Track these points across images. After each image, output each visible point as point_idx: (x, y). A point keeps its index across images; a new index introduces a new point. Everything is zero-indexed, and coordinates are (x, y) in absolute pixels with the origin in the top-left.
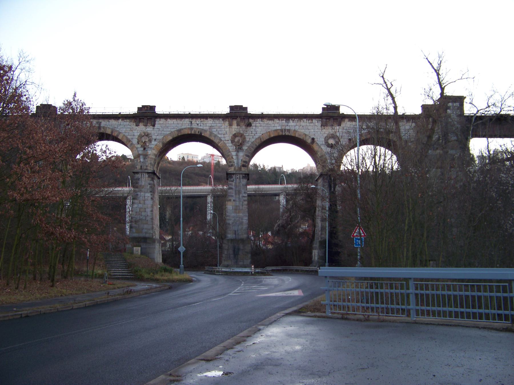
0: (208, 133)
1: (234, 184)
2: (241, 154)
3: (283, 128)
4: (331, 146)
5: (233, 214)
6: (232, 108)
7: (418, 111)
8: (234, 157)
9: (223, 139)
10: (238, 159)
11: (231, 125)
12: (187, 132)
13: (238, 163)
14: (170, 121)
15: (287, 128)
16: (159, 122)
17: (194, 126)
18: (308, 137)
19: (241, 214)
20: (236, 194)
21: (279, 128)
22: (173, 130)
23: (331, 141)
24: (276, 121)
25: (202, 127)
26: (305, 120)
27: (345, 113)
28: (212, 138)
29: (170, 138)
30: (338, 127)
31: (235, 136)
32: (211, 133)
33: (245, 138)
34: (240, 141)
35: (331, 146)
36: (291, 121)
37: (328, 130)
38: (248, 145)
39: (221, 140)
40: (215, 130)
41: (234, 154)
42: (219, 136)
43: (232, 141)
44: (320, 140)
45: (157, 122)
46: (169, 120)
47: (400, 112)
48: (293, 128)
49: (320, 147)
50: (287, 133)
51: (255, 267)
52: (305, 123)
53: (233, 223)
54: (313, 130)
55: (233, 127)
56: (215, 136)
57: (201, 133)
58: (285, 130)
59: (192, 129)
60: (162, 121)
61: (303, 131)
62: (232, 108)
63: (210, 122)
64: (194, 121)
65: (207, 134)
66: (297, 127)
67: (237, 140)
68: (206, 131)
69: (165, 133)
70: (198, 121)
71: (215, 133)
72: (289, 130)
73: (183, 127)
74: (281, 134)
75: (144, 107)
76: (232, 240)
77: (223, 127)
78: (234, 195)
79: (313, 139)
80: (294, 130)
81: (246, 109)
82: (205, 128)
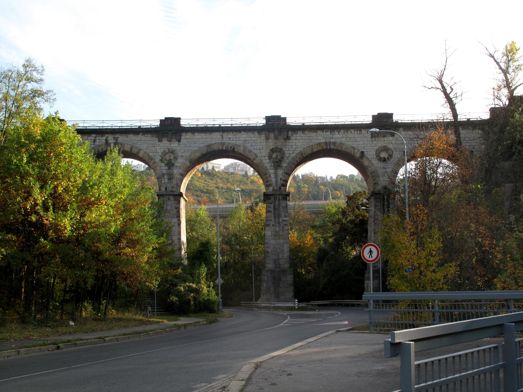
0: (242, 148)
1: (272, 206)
2: (280, 172)
3: (328, 140)
4: (384, 160)
5: (272, 242)
6: (268, 118)
7: (486, 116)
8: (272, 176)
9: (259, 155)
10: (276, 177)
11: (267, 138)
12: (216, 148)
13: (276, 182)
14: (197, 136)
15: (332, 140)
16: (185, 137)
17: (226, 140)
18: (356, 151)
19: (281, 241)
20: (275, 218)
21: (323, 141)
22: (201, 146)
23: (384, 155)
24: (320, 132)
25: (234, 142)
26: (353, 131)
27: (399, 121)
28: (247, 154)
29: (198, 155)
30: (391, 138)
31: (273, 151)
32: (245, 148)
33: (284, 154)
34: (279, 157)
35: (384, 160)
36: (336, 132)
37: (381, 142)
38: (287, 161)
39: (257, 156)
40: (250, 145)
41: (272, 171)
42: (255, 151)
43: (270, 157)
44: (370, 153)
45: (183, 137)
46: (196, 134)
47: (462, 117)
48: (338, 141)
49: (370, 161)
50: (332, 147)
51: (298, 302)
52: (353, 134)
53: (272, 251)
54: (362, 143)
55: (270, 141)
56: (250, 151)
57: (234, 149)
58: (330, 143)
59: (223, 144)
60: (189, 135)
61: (350, 144)
62: (268, 118)
63: (243, 136)
64: (225, 135)
65: (241, 150)
66: (343, 140)
67: (274, 156)
68: (239, 146)
69: (193, 149)
70: (231, 135)
71: (250, 148)
72: (334, 143)
73: (213, 142)
74: (325, 147)
75: (167, 119)
76: (272, 271)
77: (258, 141)
78: (273, 219)
79: (362, 153)
80: (341, 143)
81: (285, 119)
82: (238, 143)
